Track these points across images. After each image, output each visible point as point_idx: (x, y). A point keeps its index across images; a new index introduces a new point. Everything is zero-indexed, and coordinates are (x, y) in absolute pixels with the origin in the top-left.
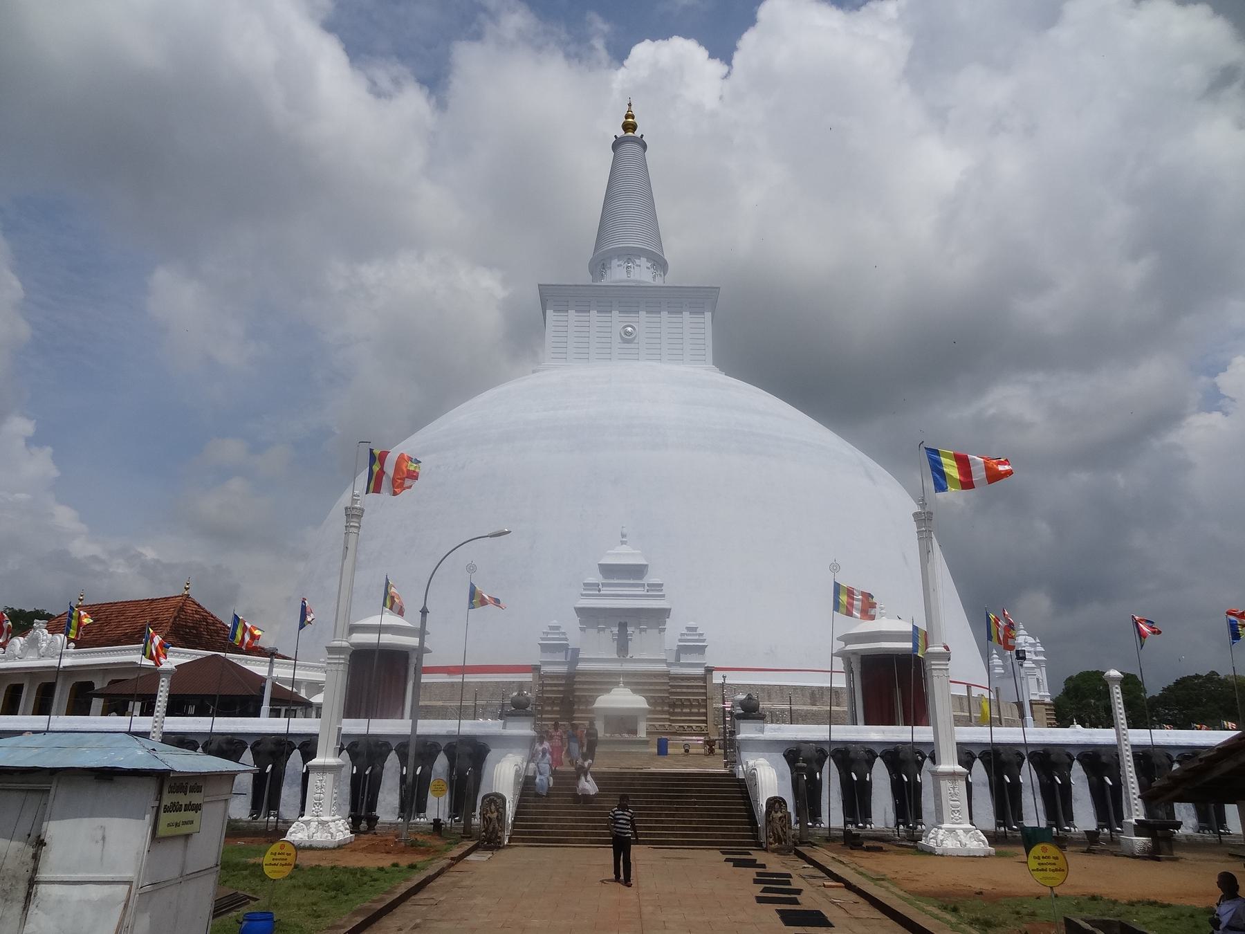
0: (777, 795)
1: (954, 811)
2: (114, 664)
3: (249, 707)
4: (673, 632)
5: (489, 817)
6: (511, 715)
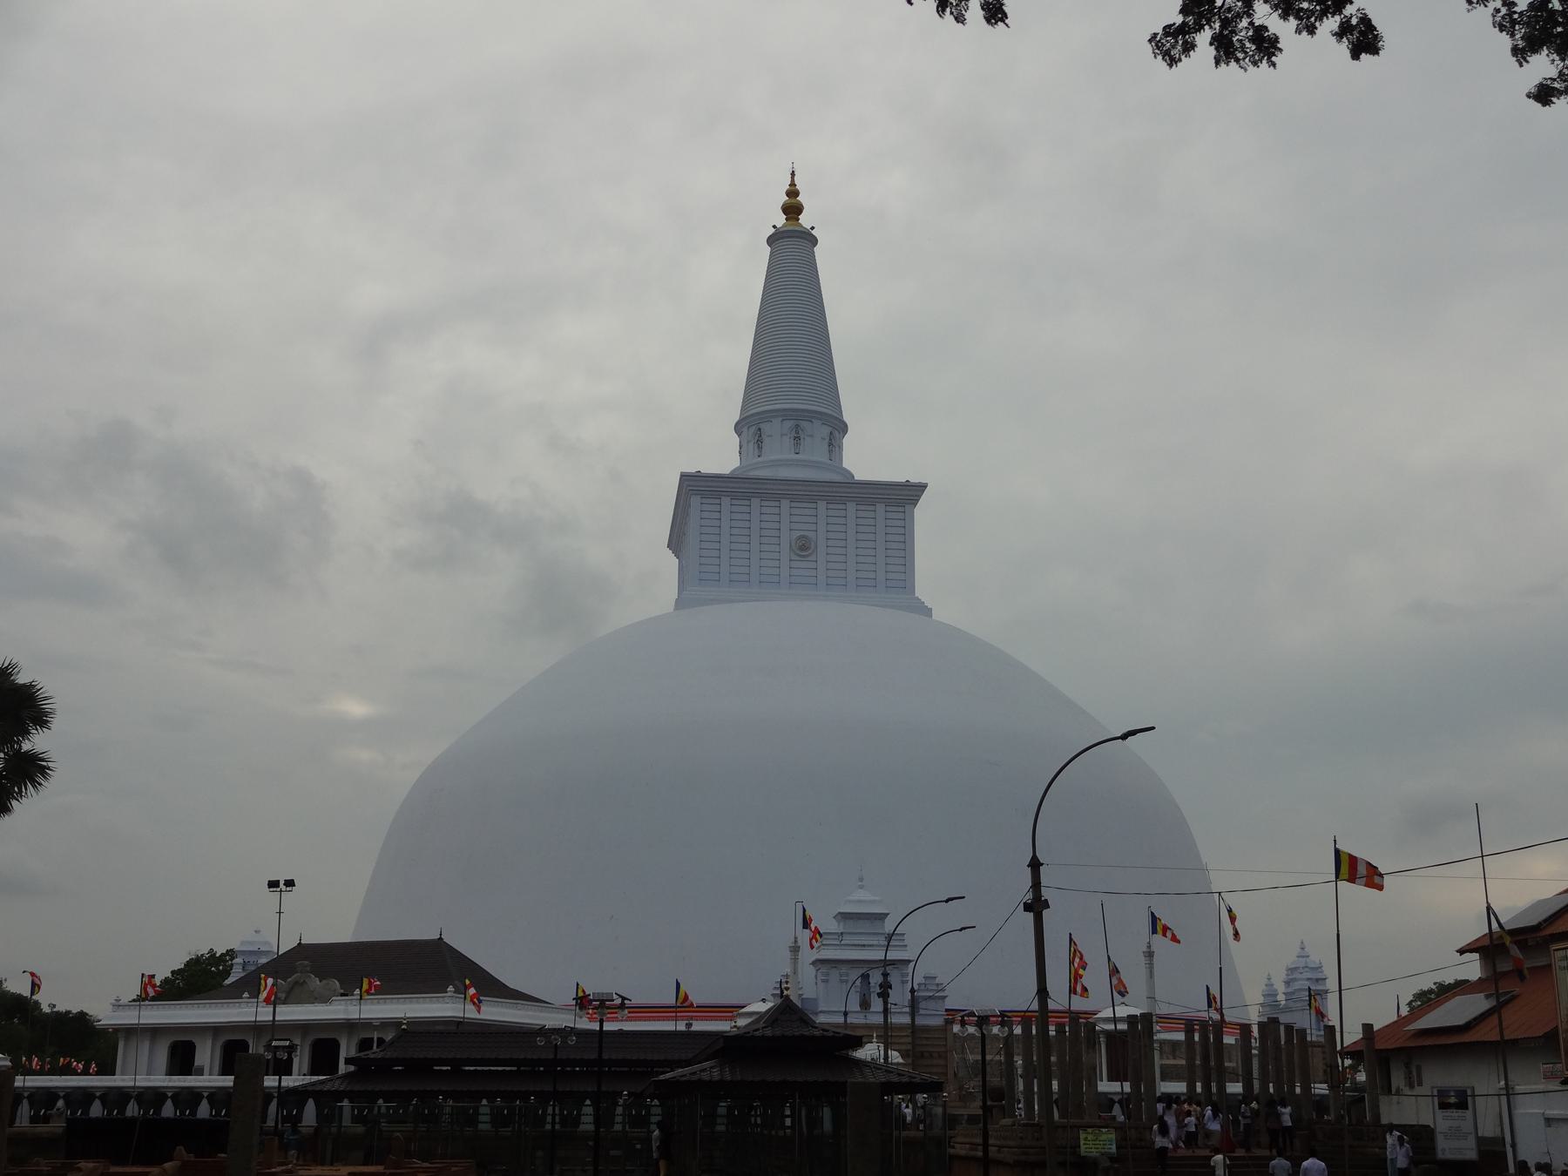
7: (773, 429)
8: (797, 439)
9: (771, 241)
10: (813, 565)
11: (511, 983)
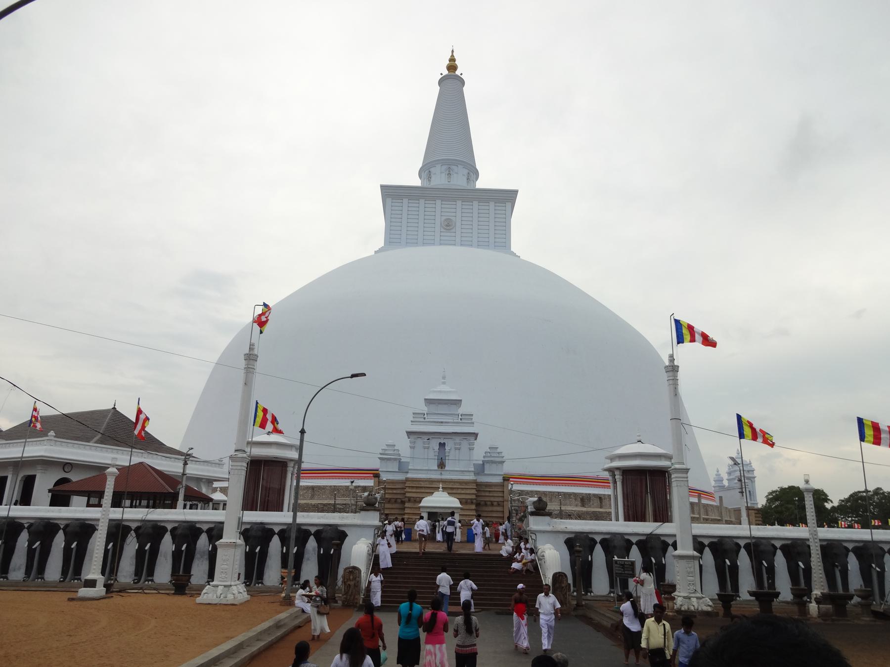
0: (560, 571)
1: (690, 584)
3: (167, 500)
4: (479, 453)
5: (349, 584)
6: (363, 509)
7: (437, 170)
8: (449, 174)
9: (441, 82)
10: (454, 234)
11: (168, 444)
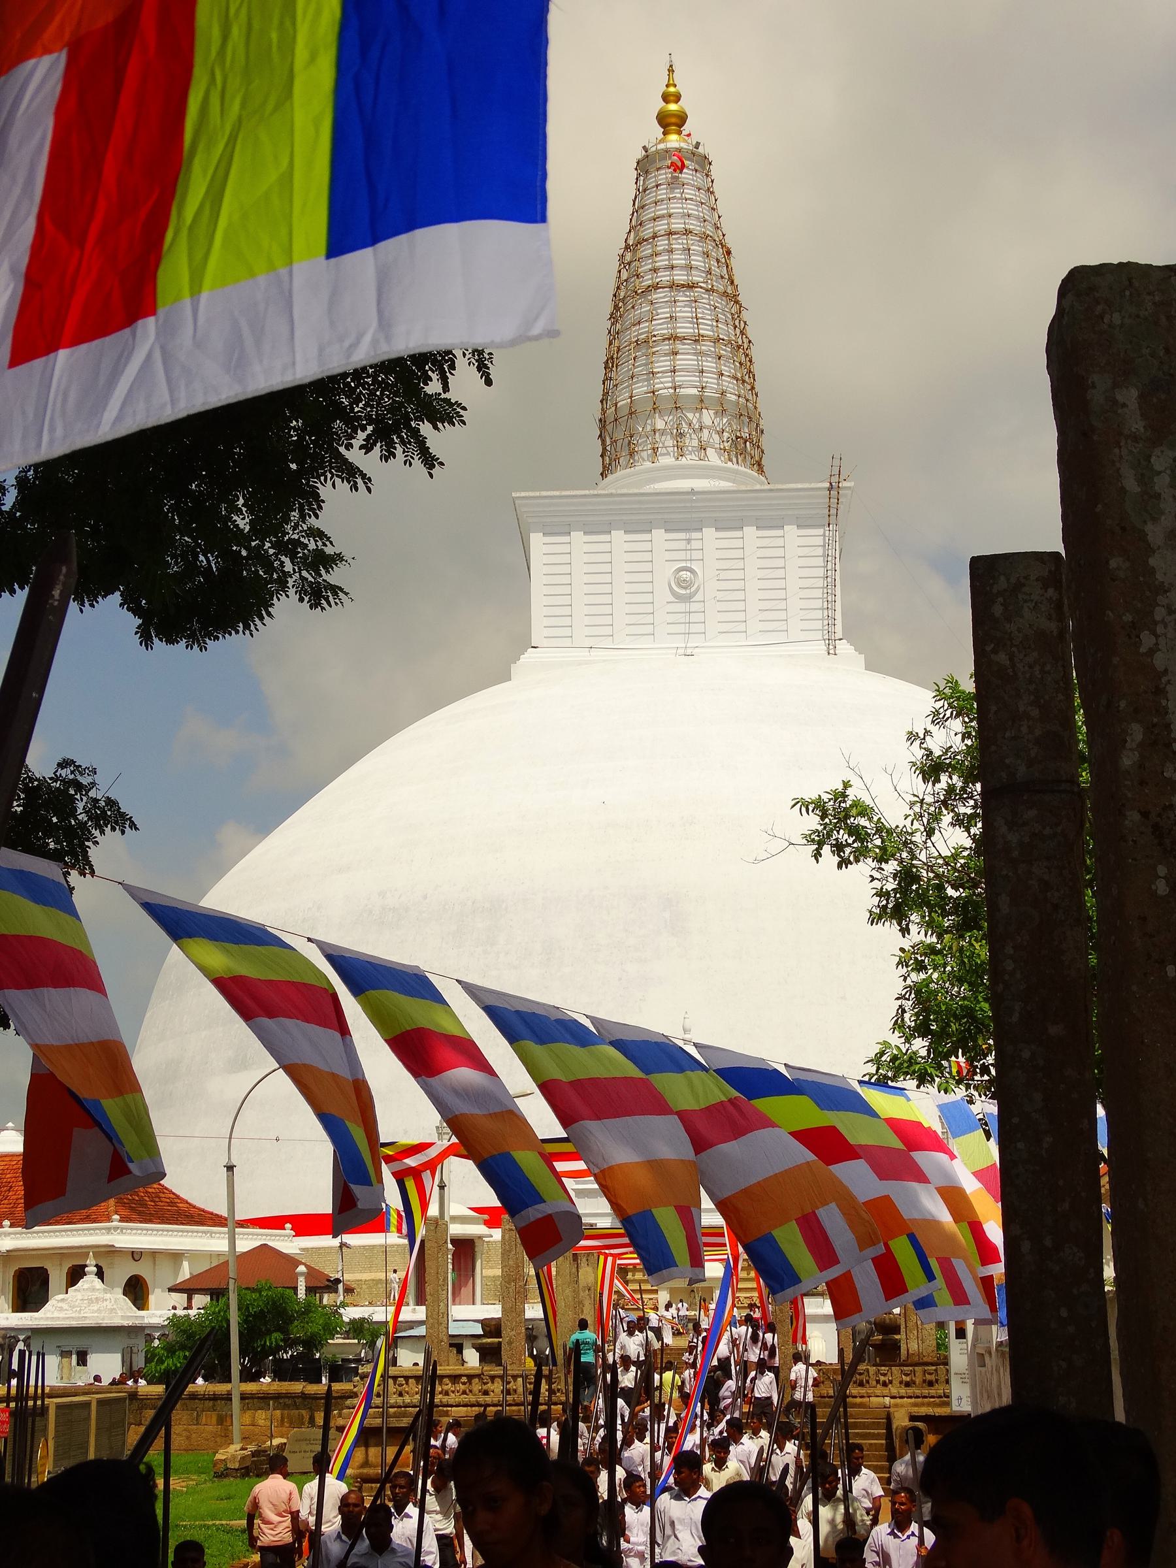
2: (81, 1247)
